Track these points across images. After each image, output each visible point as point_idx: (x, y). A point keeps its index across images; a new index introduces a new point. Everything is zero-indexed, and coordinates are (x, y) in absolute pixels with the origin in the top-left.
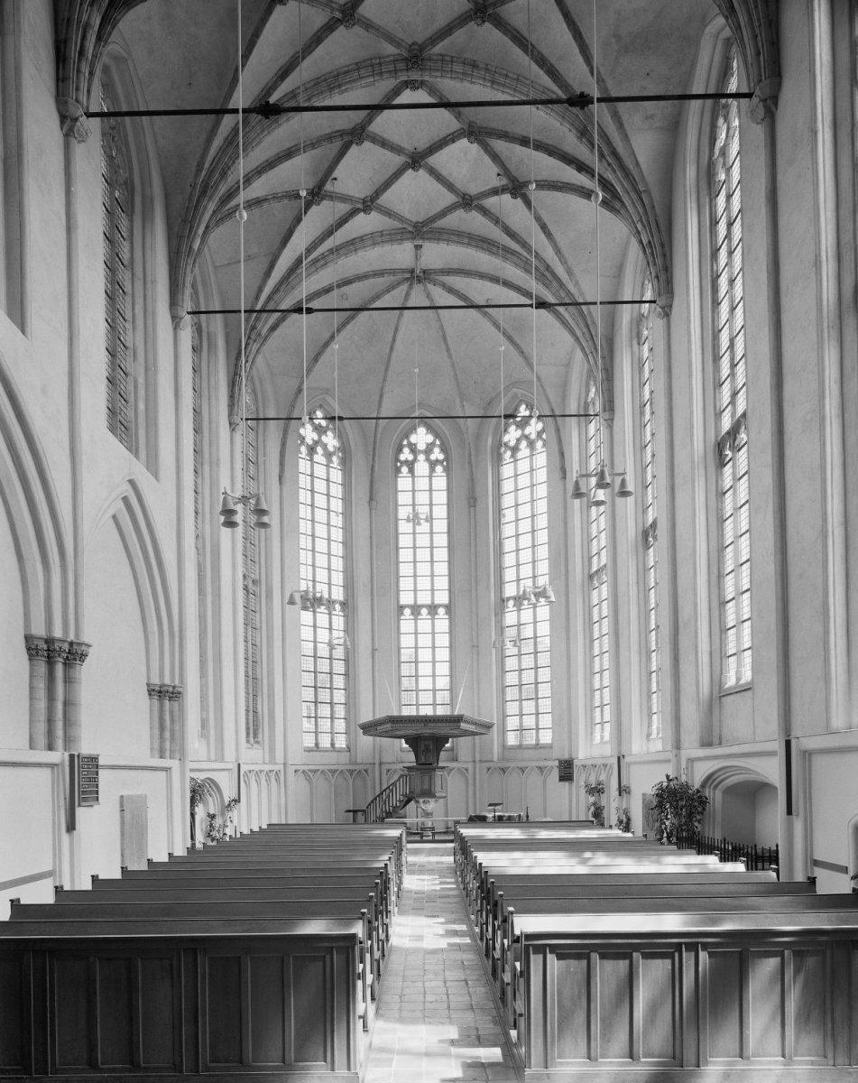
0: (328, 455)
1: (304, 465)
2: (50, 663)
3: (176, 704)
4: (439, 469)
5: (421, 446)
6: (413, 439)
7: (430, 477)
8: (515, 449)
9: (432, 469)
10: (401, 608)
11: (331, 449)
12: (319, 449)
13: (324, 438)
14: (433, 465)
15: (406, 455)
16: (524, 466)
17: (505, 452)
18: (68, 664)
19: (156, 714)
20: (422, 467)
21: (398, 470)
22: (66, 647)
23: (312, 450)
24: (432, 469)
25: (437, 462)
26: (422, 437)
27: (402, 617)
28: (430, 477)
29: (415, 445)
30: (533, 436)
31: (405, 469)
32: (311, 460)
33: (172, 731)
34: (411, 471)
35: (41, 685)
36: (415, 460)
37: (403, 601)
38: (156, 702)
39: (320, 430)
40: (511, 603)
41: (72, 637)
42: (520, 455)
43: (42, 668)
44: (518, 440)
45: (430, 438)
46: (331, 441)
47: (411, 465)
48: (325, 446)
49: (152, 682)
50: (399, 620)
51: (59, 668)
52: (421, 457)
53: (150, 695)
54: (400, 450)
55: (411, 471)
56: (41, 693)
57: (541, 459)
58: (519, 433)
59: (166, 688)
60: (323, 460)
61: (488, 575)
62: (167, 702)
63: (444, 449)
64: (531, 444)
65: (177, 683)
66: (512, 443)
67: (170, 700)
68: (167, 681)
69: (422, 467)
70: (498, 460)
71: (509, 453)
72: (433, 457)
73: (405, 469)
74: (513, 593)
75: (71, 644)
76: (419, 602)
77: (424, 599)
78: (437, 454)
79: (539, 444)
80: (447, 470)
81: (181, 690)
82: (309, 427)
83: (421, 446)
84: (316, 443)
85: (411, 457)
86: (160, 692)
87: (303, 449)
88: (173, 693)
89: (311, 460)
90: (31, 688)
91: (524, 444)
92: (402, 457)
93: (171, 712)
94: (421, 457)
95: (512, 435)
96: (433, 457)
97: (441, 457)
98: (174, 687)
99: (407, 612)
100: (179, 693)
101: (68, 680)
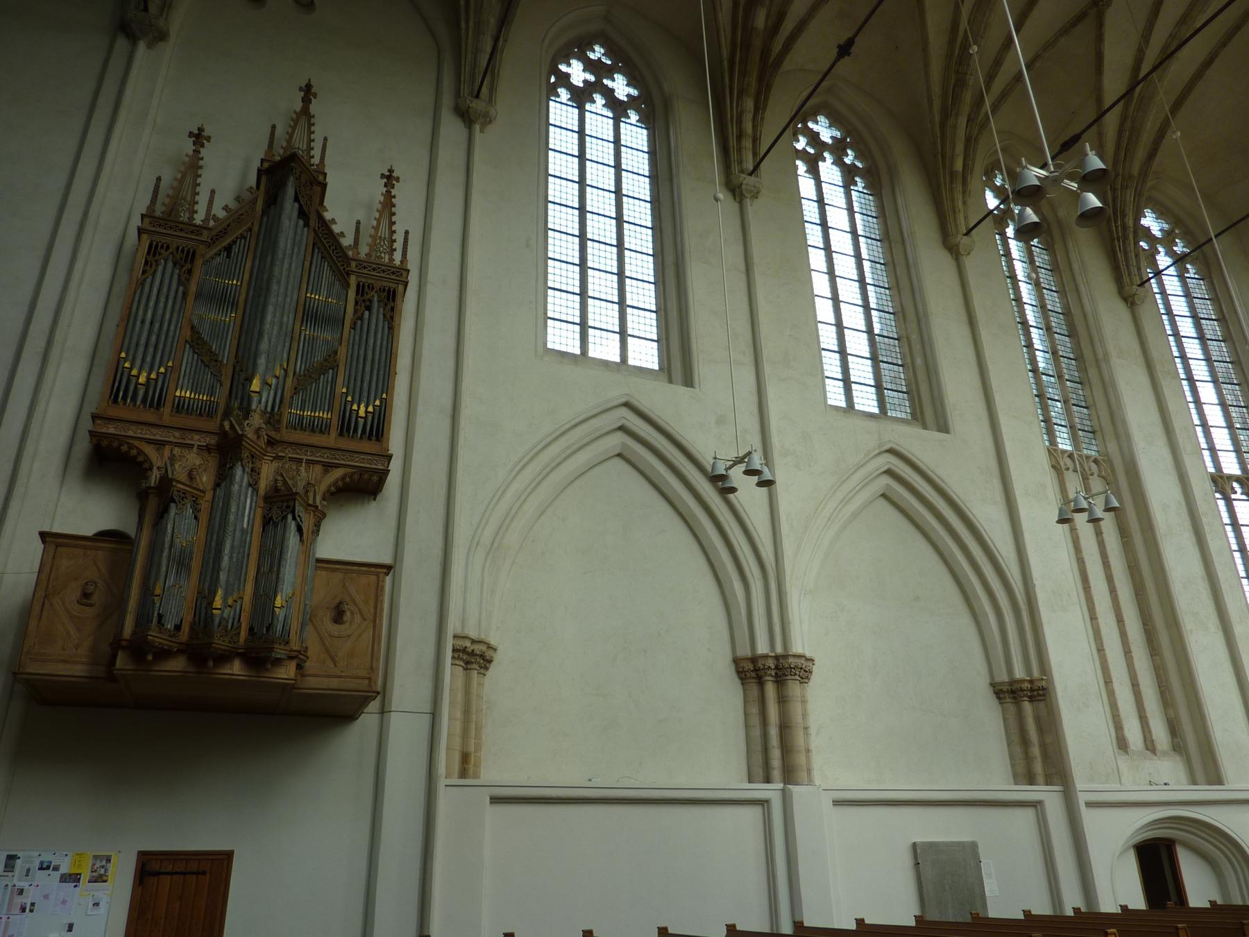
2: (761, 683)
3: (1042, 705)
18: (780, 680)
22: (771, 663)
33: (1044, 747)
35: (754, 710)
38: (1011, 708)
41: (779, 650)
43: (754, 690)
51: (770, 689)
53: (999, 698)
56: (755, 720)
62: (1027, 706)
65: (1036, 674)
68: (1019, 673)
75: (777, 658)
81: (1044, 683)
88: (1032, 690)
90: (746, 714)
93: (1037, 719)
98: (1031, 682)
100: (1043, 689)
101: (782, 700)
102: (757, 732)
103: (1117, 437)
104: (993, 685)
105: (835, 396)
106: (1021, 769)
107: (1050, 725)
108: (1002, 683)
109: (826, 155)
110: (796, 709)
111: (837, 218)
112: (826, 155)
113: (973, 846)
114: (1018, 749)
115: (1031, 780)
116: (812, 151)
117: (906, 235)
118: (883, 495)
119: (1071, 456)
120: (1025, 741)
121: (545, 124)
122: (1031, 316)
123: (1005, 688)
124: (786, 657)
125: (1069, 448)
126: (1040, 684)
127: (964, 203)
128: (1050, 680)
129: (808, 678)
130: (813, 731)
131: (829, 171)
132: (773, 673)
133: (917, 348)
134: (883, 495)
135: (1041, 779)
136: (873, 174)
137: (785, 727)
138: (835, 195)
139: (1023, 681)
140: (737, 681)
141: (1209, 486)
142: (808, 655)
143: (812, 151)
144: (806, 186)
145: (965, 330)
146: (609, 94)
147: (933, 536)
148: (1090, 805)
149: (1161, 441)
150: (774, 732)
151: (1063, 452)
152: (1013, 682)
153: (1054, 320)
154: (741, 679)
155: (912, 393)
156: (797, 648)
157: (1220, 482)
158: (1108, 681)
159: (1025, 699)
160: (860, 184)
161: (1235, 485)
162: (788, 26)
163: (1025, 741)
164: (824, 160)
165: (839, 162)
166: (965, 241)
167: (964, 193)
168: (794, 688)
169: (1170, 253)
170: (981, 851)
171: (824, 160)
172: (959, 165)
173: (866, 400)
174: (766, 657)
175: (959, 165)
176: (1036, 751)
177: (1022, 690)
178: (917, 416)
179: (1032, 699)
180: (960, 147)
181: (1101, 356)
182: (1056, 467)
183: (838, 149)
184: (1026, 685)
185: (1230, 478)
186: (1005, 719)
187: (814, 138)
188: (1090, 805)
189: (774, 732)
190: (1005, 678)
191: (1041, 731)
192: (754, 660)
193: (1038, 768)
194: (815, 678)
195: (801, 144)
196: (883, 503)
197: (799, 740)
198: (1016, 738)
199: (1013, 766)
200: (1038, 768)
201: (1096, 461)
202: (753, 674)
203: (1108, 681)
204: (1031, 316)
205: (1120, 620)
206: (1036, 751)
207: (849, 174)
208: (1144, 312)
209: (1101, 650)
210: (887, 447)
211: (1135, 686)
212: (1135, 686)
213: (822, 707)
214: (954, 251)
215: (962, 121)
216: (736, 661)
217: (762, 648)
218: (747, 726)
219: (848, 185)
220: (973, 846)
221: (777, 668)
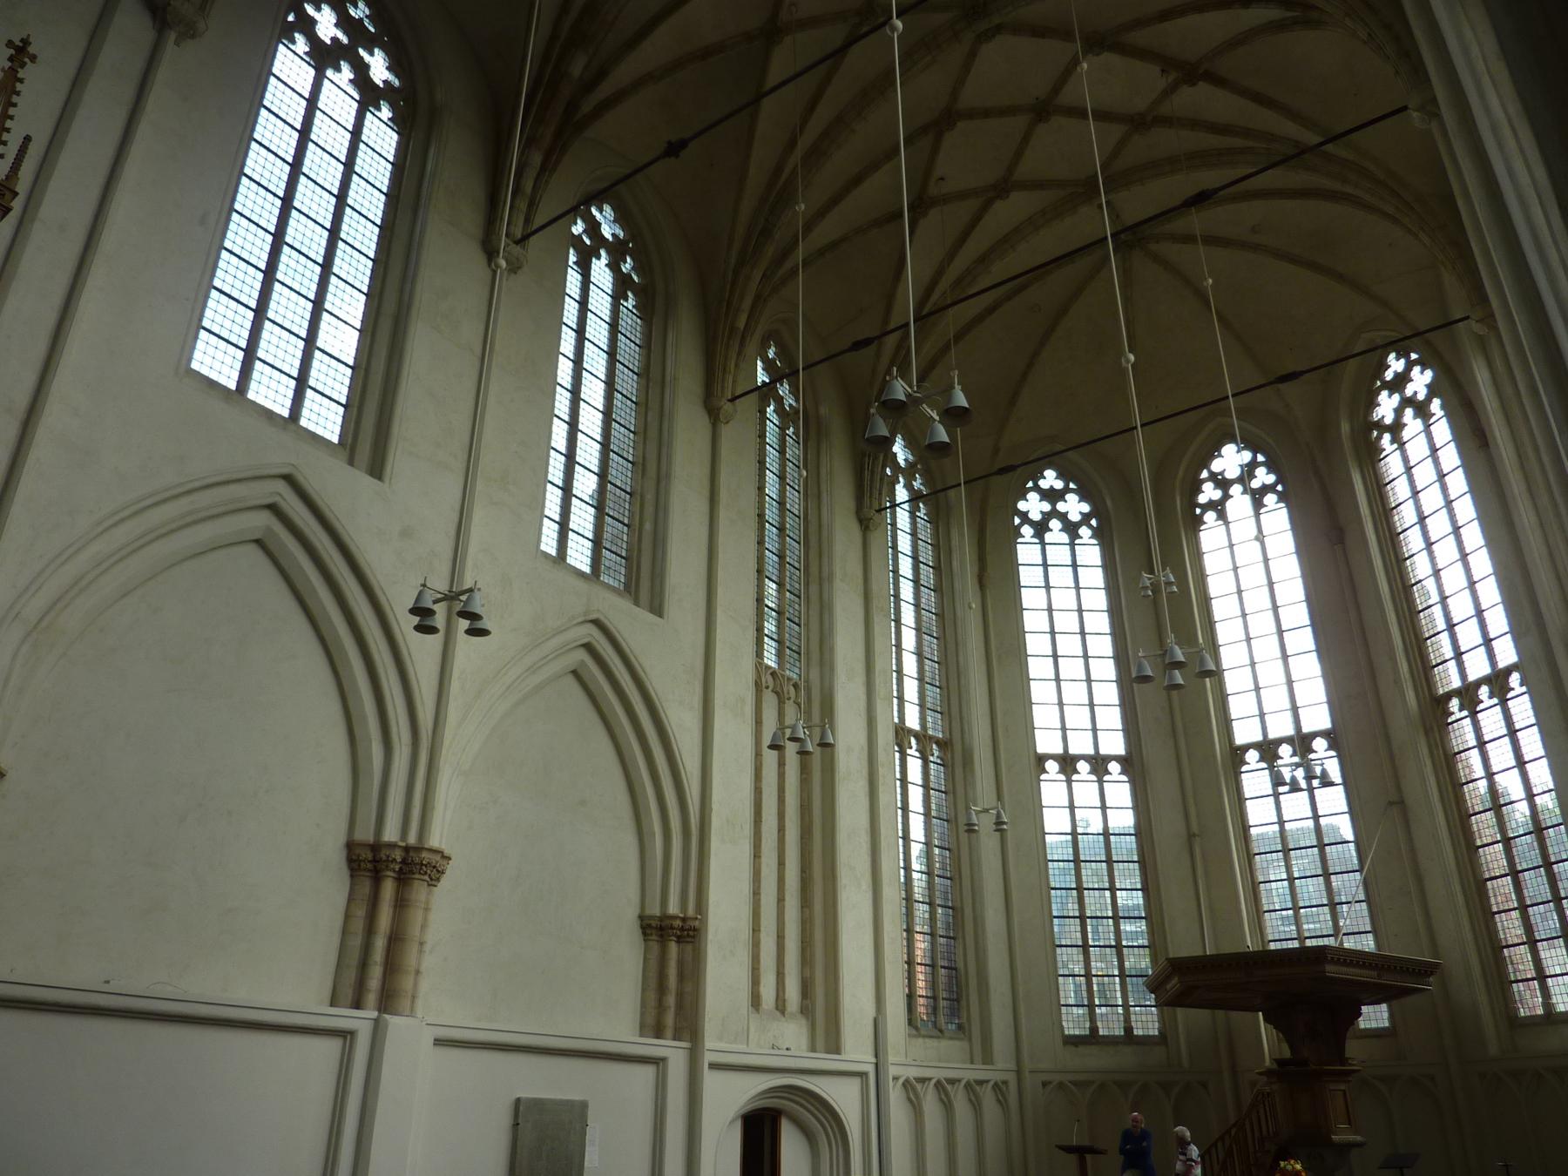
0: (1071, 529)
1: (1027, 552)
2: (377, 880)
3: (689, 948)
4: (1270, 499)
5: (1233, 473)
6: (1216, 466)
7: (1257, 515)
8: (1396, 428)
9: (1258, 504)
10: (1237, 755)
11: (1075, 517)
12: (1055, 524)
13: (1061, 507)
14: (1257, 497)
15: (1209, 493)
16: (1417, 448)
17: (1380, 437)
18: (403, 879)
19: (653, 964)
20: (1239, 503)
21: (1199, 521)
22: (398, 855)
23: (1041, 528)
24: (1258, 504)
25: (1266, 489)
26: (1230, 459)
27: (1244, 769)
28: (1257, 515)
29: (1222, 473)
30: (1421, 397)
31: (1210, 517)
32: (1043, 544)
33: (680, 996)
34: (1222, 515)
35: (360, 912)
36: (1226, 496)
37: (1240, 738)
38: (655, 947)
39: (1052, 496)
40: (1454, 703)
41: (412, 840)
42: (1406, 434)
43: (365, 887)
44: (1399, 412)
45: (1247, 456)
46: (1074, 507)
47: (1218, 507)
48: (1063, 517)
49: (648, 912)
50: (1237, 774)
51: (388, 888)
52: (1236, 490)
53: (644, 934)
54: (1198, 490)
55: (1222, 515)
56: (358, 925)
57: (1442, 430)
58: (1396, 398)
59: (668, 922)
60: (1065, 538)
61: (1393, 659)
62: (673, 947)
63: (1271, 466)
64: (1422, 410)
65: (691, 912)
66: (1388, 420)
67: (678, 942)
68: (673, 908)
69: (1239, 503)
70: (1372, 454)
71: (1387, 437)
72: (1255, 484)
73: (1210, 517)
74: (1456, 683)
75: (407, 849)
76: (1272, 736)
77: (1281, 727)
78: (1263, 477)
79: (1436, 406)
80: (1282, 497)
81: (697, 923)
82: (1033, 497)
83: (1233, 473)
84: (1047, 517)
85: (1217, 495)
86: (661, 928)
87: (1027, 531)
88: (682, 929)
89: (1043, 544)
90: (348, 916)
91: (1409, 412)
92: (1202, 499)
94: (1236, 490)
95: (1386, 406)
96: (1255, 484)
97: (1271, 479)
98: (684, 920)
99: (1252, 756)
101: (401, 904)
102: (356, 942)
103: (822, 663)
104: (641, 918)
105: (549, 544)
106: (650, 1020)
107: (692, 972)
108: (652, 917)
109: (603, 252)
110: (415, 917)
111: (598, 331)
112: (603, 252)
113: (584, 1106)
114: (652, 996)
115: (658, 1033)
116: (588, 242)
117: (668, 379)
118: (575, 673)
119: (774, 674)
120: (662, 989)
121: (262, 73)
122: (771, 513)
123: (654, 923)
124: (419, 849)
125: (773, 665)
126: (692, 923)
127: (737, 365)
128: (704, 921)
129: (438, 880)
130: (427, 948)
131: (600, 270)
132: (397, 868)
133: (649, 509)
134: (575, 673)
135: (669, 1032)
136: (645, 292)
137: (396, 939)
138: (600, 302)
139: (675, 917)
140: (345, 873)
141: (891, 735)
142: (447, 853)
143: (588, 242)
144: (573, 280)
145: (704, 507)
146: (361, 70)
147: (617, 731)
148: (713, 1066)
149: (860, 679)
150: (380, 943)
151: (768, 667)
152: (665, 917)
153: (790, 521)
154: (352, 869)
155: (631, 561)
156: (434, 841)
157: (901, 733)
158: (756, 929)
159: (672, 936)
160: (630, 302)
161: (913, 741)
162: (605, 89)
163: (662, 989)
164: (599, 258)
165: (614, 266)
166: (728, 407)
167: (739, 354)
168: (419, 891)
169: (909, 487)
170: (590, 1113)
171: (599, 258)
172: (741, 323)
173: (580, 555)
174: (392, 846)
175: (741, 323)
176: (671, 1000)
177: (672, 928)
178: (631, 589)
179: (679, 940)
180: (747, 304)
181: (825, 574)
182: (758, 686)
183: (617, 252)
184: (678, 923)
185: (910, 731)
186: (645, 959)
187: (593, 227)
188: (713, 1066)
189: (380, 943)
190: (657, 912)
191: (681, 976)
192: (376, 847)
193: (670, 1019)
194: (445, 882)
195: (578, 228)
196: (571, 682)
197: (411, 958)
198: (653, 983)
199: (643, 1014)
200: (670, 1019)
201: (796, 686)
202: (369, 866)
203: (756, 929)
204: (771, 513)
205: (781, 864)
206: (671, 1000)
207: (621, 286)
208: (875, 536)
209: (756, 893)
210: (594, 616)
211: (780, 938)
212: (780, 938)
213: (442, 915)
214: (714, 415)
215: (757, 275)
216: (350, 846)
217: (391, 834)
218: (345, 932)
219: (617, 297)
220: (584, 1106)
221: (404, 861)
